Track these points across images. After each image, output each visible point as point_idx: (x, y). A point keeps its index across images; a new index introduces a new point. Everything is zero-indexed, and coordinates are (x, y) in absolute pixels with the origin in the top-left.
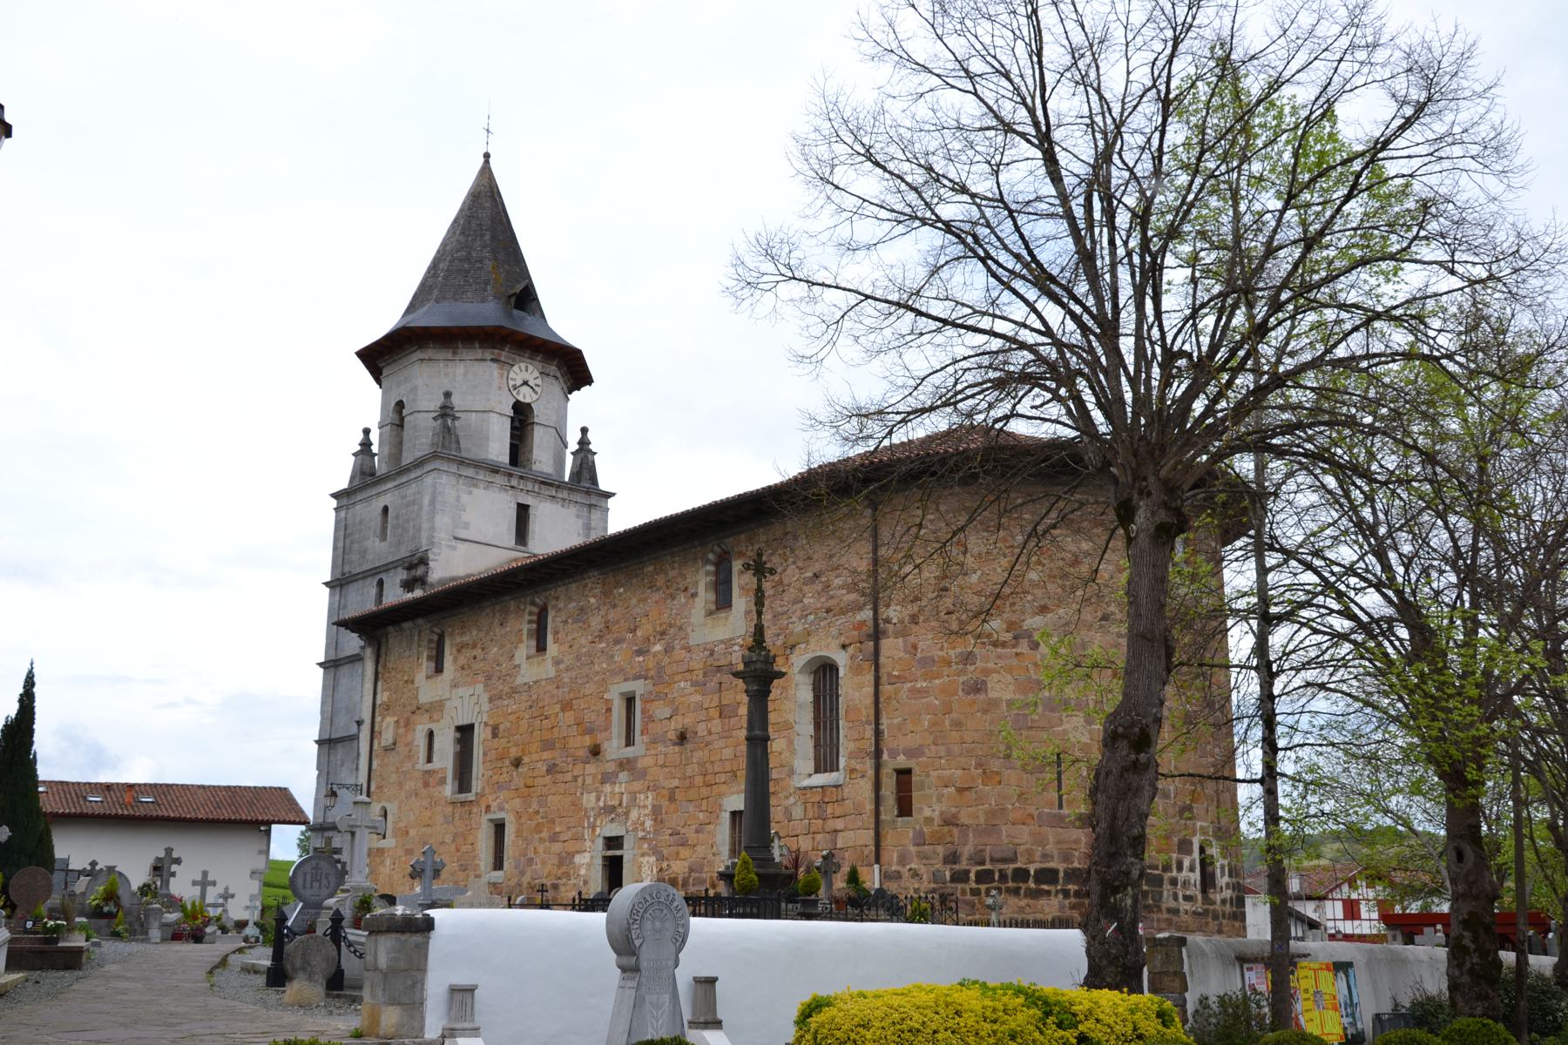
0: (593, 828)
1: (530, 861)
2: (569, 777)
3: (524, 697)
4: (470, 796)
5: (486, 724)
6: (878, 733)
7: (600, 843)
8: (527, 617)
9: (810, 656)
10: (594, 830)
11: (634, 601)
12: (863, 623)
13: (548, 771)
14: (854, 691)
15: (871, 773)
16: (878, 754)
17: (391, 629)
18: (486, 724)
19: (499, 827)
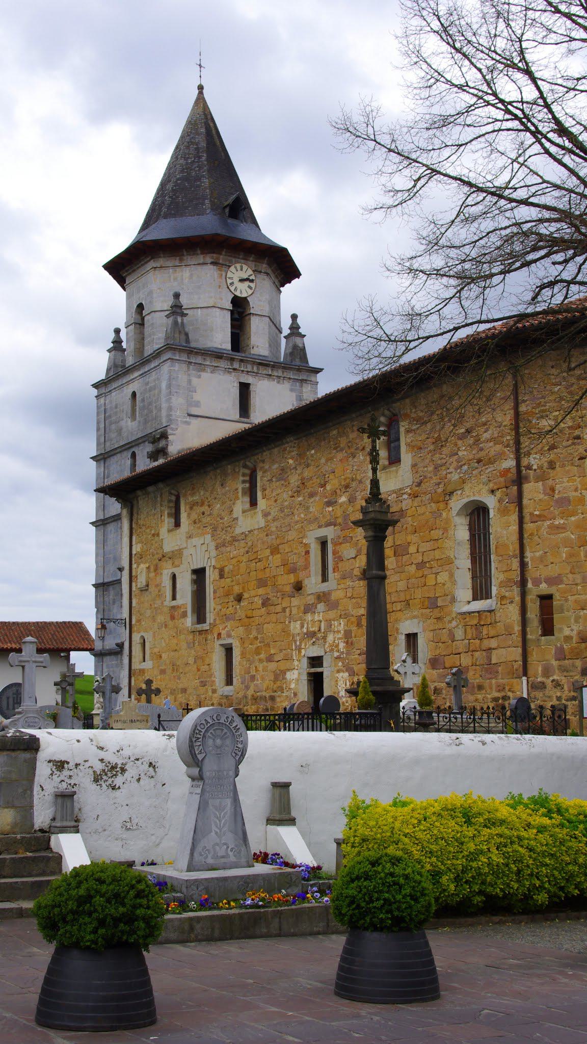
0: (299, 649)
1: (253, 678)
2: (279, 609)
3: (242, 543)
4: (205, 626)
5: (214, 567)
6: (523, 565)
7: (305, 662)
8: (241, 478)
9: (466, 500)
10: (300, 652)
11: (323, 461)
12: (508, 470)
13: (264, 604)
14: (502, 529)
15: (518, 599)
16: (523, 583)
17: (139, 493)
18: (214, 567)
19: (229, 650)
